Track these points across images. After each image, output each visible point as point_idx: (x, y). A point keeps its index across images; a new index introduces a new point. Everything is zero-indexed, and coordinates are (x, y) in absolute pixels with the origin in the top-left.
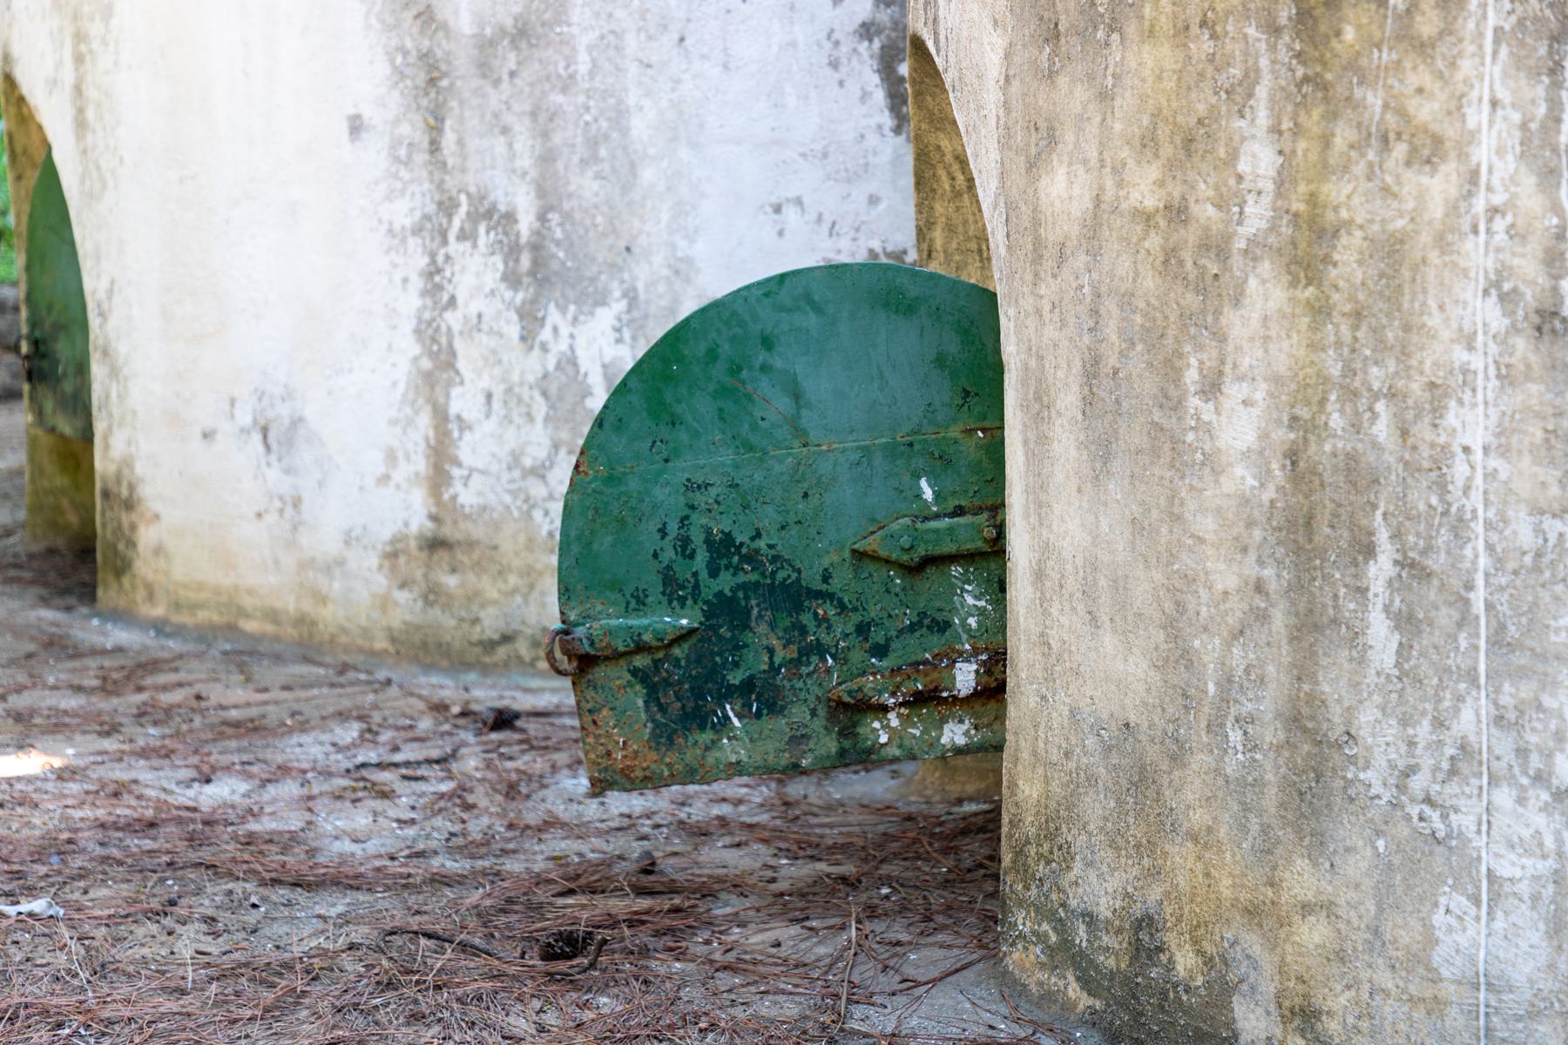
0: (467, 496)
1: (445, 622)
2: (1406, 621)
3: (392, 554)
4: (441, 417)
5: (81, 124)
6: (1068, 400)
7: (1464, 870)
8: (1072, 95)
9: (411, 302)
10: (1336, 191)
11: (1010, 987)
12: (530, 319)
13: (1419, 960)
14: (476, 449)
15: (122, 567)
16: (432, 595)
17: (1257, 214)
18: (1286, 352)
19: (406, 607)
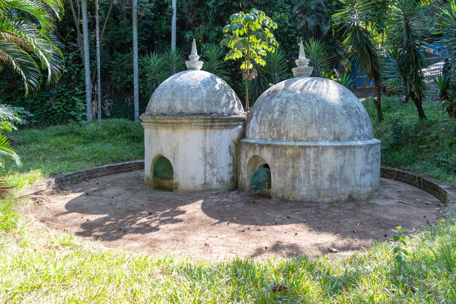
0: (207, 181)
1: (205, 189)
2: (299, 181)
3: (202, 185)
4: (205, 176)
5: (174, 159)
6: (277, 173)
7: (302, 191)
8: (277, 160)
9: (204, 169)
10: (295, 165)
11: (274, 201)
12: (211, 169)
13: (300, 195)
14: (207, 178)
15: (176, 188)
16: (204, 187)
17: (290, 166)
18: (292, 171)
19: (203, 188)
